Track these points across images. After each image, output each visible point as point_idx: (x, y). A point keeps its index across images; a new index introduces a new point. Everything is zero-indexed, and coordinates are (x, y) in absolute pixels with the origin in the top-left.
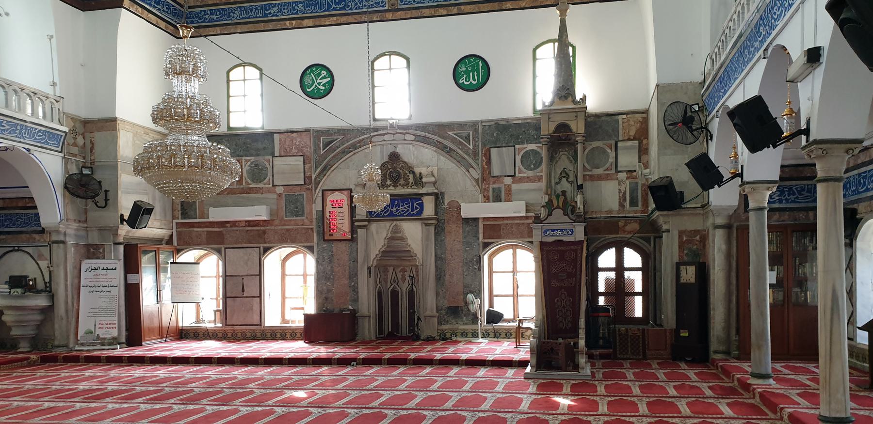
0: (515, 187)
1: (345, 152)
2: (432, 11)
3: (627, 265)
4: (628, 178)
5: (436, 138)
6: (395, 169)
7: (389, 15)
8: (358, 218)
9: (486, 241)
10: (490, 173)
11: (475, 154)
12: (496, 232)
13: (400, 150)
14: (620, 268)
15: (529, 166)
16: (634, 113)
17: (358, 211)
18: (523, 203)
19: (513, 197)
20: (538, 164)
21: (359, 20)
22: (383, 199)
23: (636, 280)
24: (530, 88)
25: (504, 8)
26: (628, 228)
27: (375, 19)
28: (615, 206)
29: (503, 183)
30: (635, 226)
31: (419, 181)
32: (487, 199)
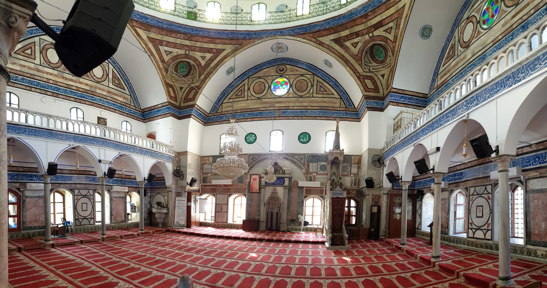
3: (351, 205)
6: (277, 168)
11: (304, 165)
12: (310, 192)
13: (278, 161)
14: (349, 207)
16: (357, 156)
18: (320, 182)
20: (325, 169)
22: (274, 179)
23: (353, 210)
24: (325, 145)
26: (353, 193)
28: (349, 185)
30: (355, 192)
31: (284, 172)
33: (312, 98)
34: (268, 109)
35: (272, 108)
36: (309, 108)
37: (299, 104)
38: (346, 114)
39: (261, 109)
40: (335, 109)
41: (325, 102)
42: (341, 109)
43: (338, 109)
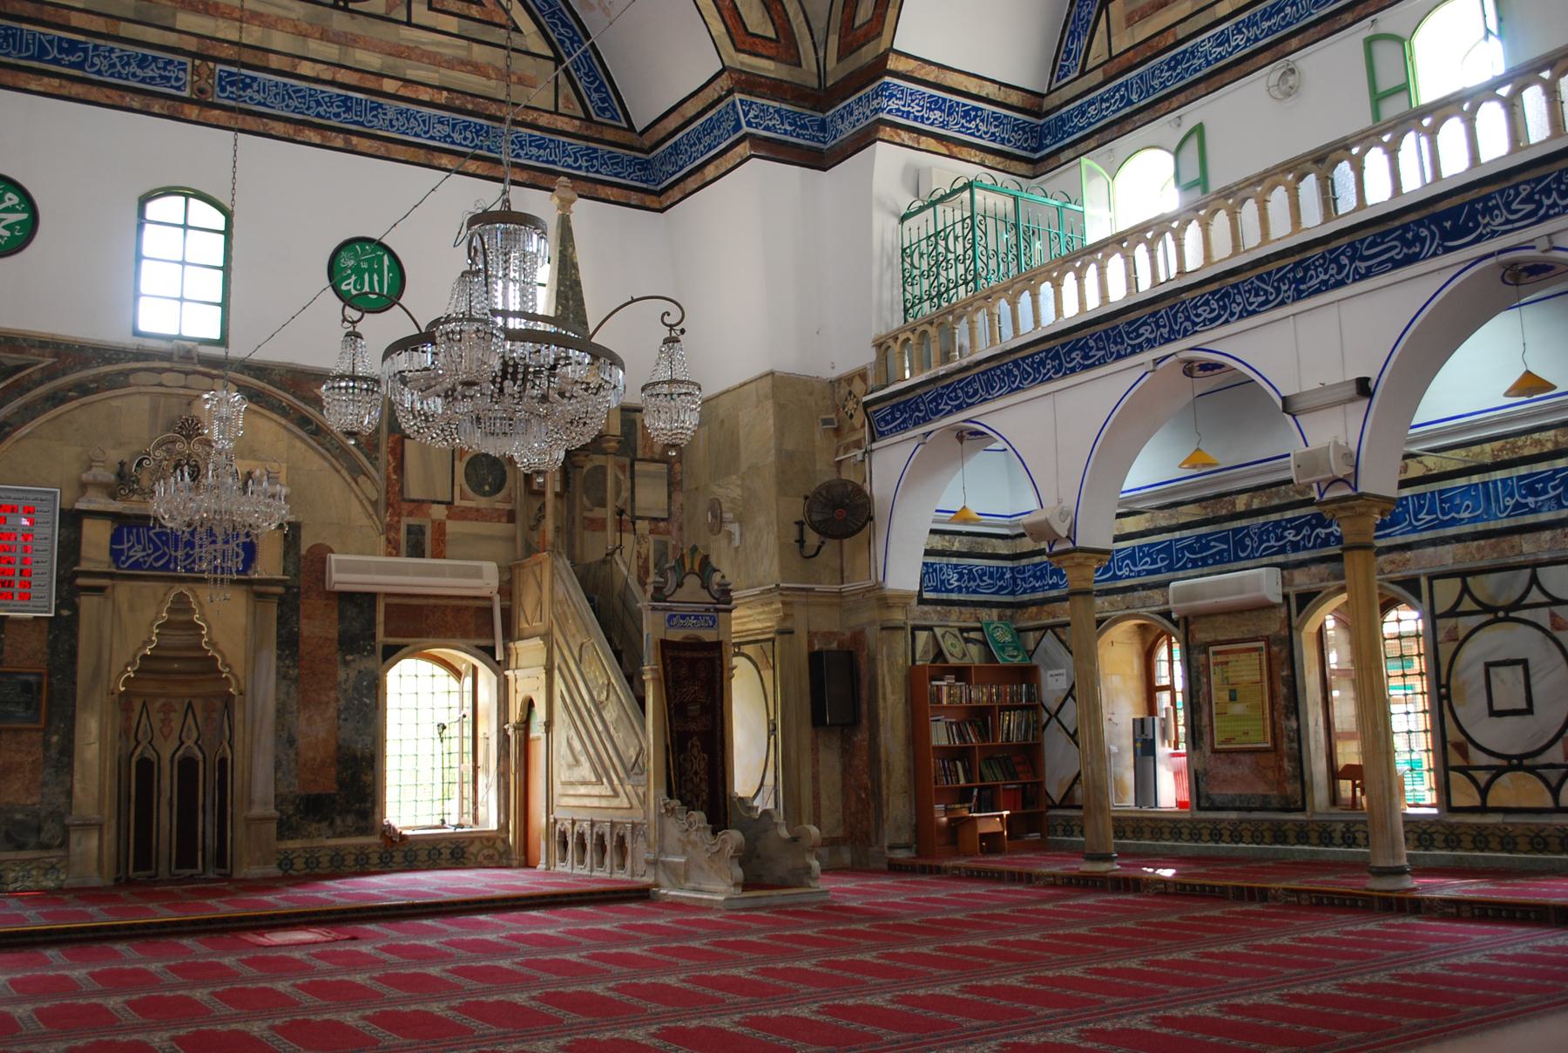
0: (452, 527)
1: (56, 399)
2: (290, 130)
4: (651, 532)
5: (287, 398)
7: (193, 112)
8: (84, 566)
9: (392, 641)
10: (401, 490)
15: (482, 486)
17: (86, 550)
19: (449, 550)
21: (118, 101)
25: (436, 163)
27: (156, 109)
29: (429, 516)
32: (393, 548)
33: (407, 32)
34: (127, 30)
35: (152, 35)
36: (389, 86)
37: (331, 52)
38: (591, 155)
39: (77, 20)
40: (530, 117)
41: (477, 69)
42: (561, 123)
43: (544, 120)
